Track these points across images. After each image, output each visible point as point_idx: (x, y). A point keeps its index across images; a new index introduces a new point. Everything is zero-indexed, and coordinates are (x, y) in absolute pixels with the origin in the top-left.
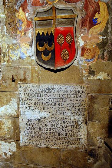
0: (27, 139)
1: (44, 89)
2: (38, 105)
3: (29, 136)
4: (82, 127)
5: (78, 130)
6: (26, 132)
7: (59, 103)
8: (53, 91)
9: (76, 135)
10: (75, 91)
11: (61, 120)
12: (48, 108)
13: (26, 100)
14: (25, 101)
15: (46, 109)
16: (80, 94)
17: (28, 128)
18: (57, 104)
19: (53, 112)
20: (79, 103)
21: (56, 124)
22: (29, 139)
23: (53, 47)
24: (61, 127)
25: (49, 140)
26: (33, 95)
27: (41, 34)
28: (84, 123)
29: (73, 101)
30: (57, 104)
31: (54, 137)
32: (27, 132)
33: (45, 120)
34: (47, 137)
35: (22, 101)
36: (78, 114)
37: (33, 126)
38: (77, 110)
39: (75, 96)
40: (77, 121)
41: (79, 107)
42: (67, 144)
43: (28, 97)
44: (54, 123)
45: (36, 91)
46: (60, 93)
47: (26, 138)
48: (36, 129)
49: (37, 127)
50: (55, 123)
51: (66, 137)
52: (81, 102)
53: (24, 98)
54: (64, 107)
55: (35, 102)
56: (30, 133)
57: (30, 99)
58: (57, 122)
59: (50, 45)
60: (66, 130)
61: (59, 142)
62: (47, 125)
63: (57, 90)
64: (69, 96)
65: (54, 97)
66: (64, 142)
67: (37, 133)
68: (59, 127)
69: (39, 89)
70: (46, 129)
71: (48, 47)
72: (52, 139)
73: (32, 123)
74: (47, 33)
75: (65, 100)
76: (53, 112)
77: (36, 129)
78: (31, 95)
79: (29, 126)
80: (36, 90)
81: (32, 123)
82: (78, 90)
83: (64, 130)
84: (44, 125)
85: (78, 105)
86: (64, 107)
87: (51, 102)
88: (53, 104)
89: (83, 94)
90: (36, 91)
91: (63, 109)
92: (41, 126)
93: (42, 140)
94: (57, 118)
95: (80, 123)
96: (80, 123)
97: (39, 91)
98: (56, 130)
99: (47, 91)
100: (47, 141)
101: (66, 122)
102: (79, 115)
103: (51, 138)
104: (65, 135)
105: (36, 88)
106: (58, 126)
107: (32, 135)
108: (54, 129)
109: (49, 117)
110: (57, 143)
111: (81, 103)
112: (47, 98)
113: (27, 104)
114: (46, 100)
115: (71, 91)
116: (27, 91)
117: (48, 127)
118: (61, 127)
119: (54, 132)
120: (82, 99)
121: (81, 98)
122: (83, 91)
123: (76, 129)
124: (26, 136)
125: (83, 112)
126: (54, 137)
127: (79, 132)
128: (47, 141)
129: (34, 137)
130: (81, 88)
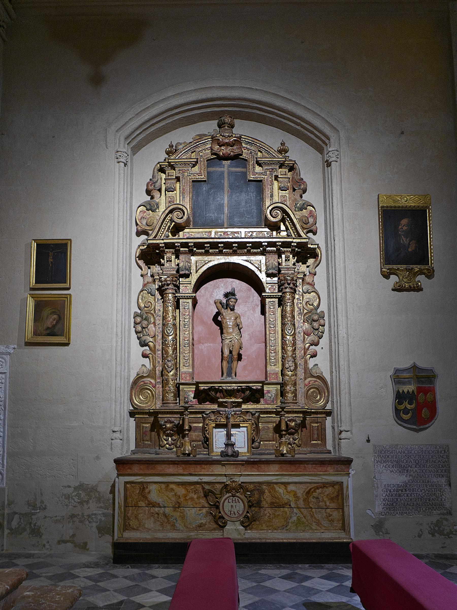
0: (383, 508)
1: (402, 450)
2: (397, 467)
3: (386, 505)
4: (446, 490)
5: (442, 493)
6: (382, 500)
7: (419, 464)
8: (413, 452)
9: (440, 499)
10: (436, 452)
11: (423, 483)
12: (407, 471)
13: (382, 462)
14: (381, 464)
15: (406, 471)
16: (442, 455)
17: (384, 495)
18: (418, 466)
19: (414, 475)
20: (442, 464)
21: (417, 488)
22: (385, 509)
23: (413, 406)
24: (423, 491)
25: (410, 507)
26: (390, 456)
27: (401, 391)
28: (448, 485)
29: (435, 462)
30: (418, 466)
31: (415, 503)
32: (384, 500)
33: (405, 484)
34: (408, 504)
35: (377, 464)
36: (441, 476)
37: (390, 491)
38: (440, 471)
39: (437, 456)
40: (440, 484)
41: (442, 468)
42: (430, 510)
43: (384, 459)
44: (416, 487)
45: (394, 453)
46: (421, 454)
47: (383, 507)
48: (394, 495)
49: (395, 493)
50: (416, 487)
51: (429, 502)
52: (444, 463)
53: (380, 461)
54: (426, 469)
55: (392, 464)
56: (387, 501)
57: (387, 461)
58: (418, 486)
59: (410, 404)
60: (429, 494)
61: (421, 508)
62: (407, 490)
63: (418, 450)
64: (430, 457)
65: (414, 459)
66: (427, 508)
67: (395, 500)
68: (421, 491)
69: (398, 450)
70: (405, 495)
71: (409, 407)
72: (413, 506)
73: (390, 488)
74: (408, 391)
75: (427, 461)
76: (414, 475)
77: (394, 495)
78: (388, 457)
79: (386, 493)
80: (394, 451)
81: (390, 488)
82: (439, 450)
83: (427, 494)
84: (404, 490)
85: (441, 466)
86: (426, 469)
87: (410, 464)
88: (414, 466)
89: (445, 454)
90: (394, 453)
91: (424, 471)
92: (400, 492)
93: (402, 508)
94: (419, 482)
95: (443, 486)
96: (443, 486)
97: (397, 452)
98: (418, 495)
99: (406, 452)
100: (408, 509)
101: (428, 485)
102: (443, 476)
103: (412, 504)
104: (427, 500)
105: (394, 449)
106: (419, 490)
107: (389, 504)
108: (415, 495)
109: (409, 481)
110: (419, 510)
111: (444, 464)
112: (407, 459)
113: (384, 468)
114: (405, 461)
115: (433, 452)
116: (383, 452)
117: (408, 492)
118: (423, 491)
119: (415, 497)
120: (444, 459)
121: (443, 459)
122: (445, 451)
123: (440, 493)
124: (382, 504)
125: (446, 474)
126: (415, 503)
127: (443, 496)
128: (408, 509)
129: (392, 505)
130: (443, 448)
